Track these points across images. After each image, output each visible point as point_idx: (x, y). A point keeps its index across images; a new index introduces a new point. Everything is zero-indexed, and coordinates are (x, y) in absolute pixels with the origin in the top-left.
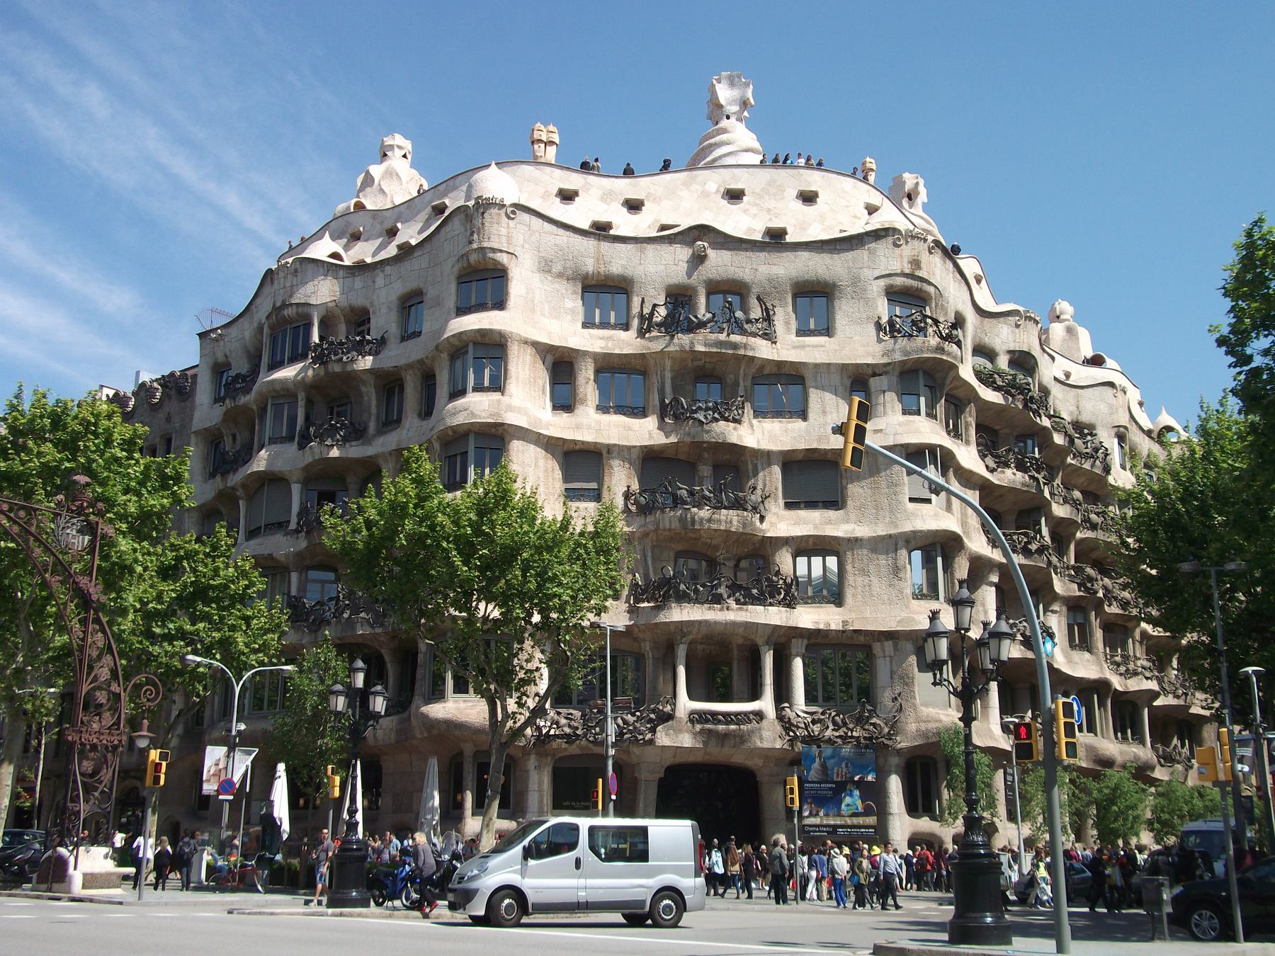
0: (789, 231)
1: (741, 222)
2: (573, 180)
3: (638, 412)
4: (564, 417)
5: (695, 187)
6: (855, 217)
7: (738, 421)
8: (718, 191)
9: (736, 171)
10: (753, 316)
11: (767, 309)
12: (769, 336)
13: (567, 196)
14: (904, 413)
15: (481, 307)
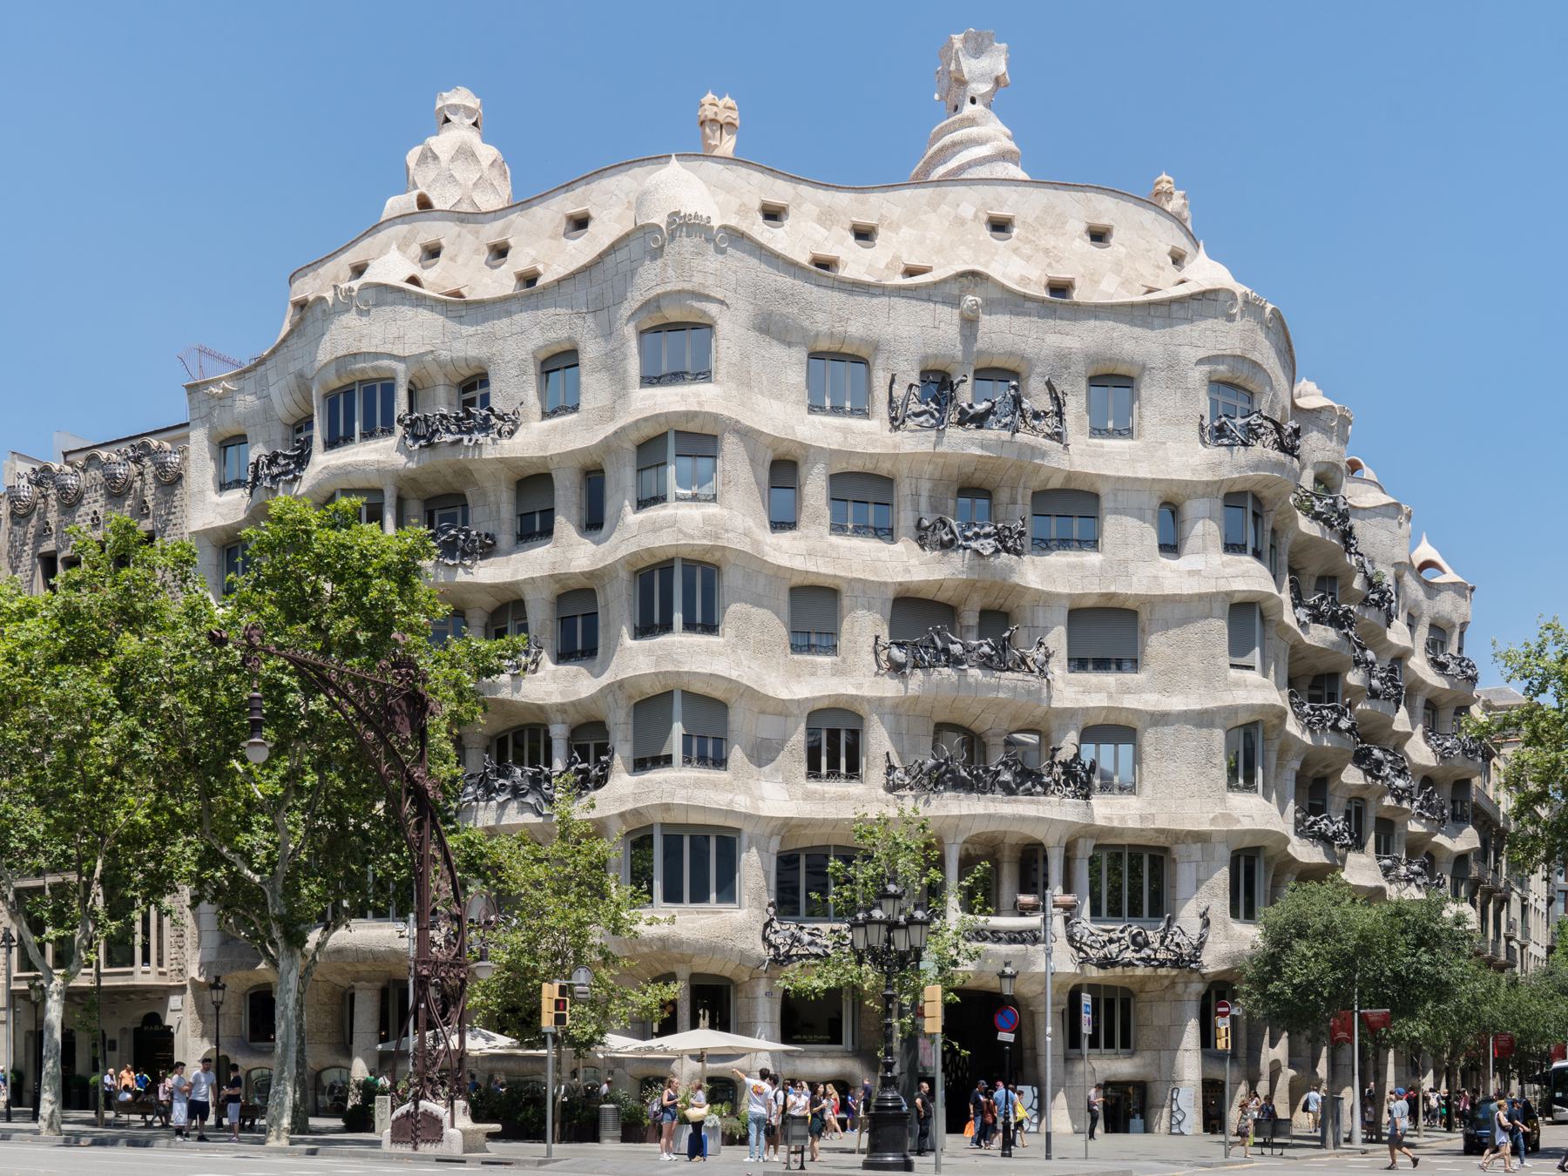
0: (1077, 284)
1: (1015, 267)
2: (778, 191)
3: (886, 533)
4: (785, 539)
5: (944, 208)
6: (1158, 267)
7: (1018, 553)
8: (976, 217)
9: (1002, 189)
10: (1038, 408)
11: (1057, 398)
12: (1058, 436)
13: (773, 214)
14: (1231, 547)
15: (677, 377)
